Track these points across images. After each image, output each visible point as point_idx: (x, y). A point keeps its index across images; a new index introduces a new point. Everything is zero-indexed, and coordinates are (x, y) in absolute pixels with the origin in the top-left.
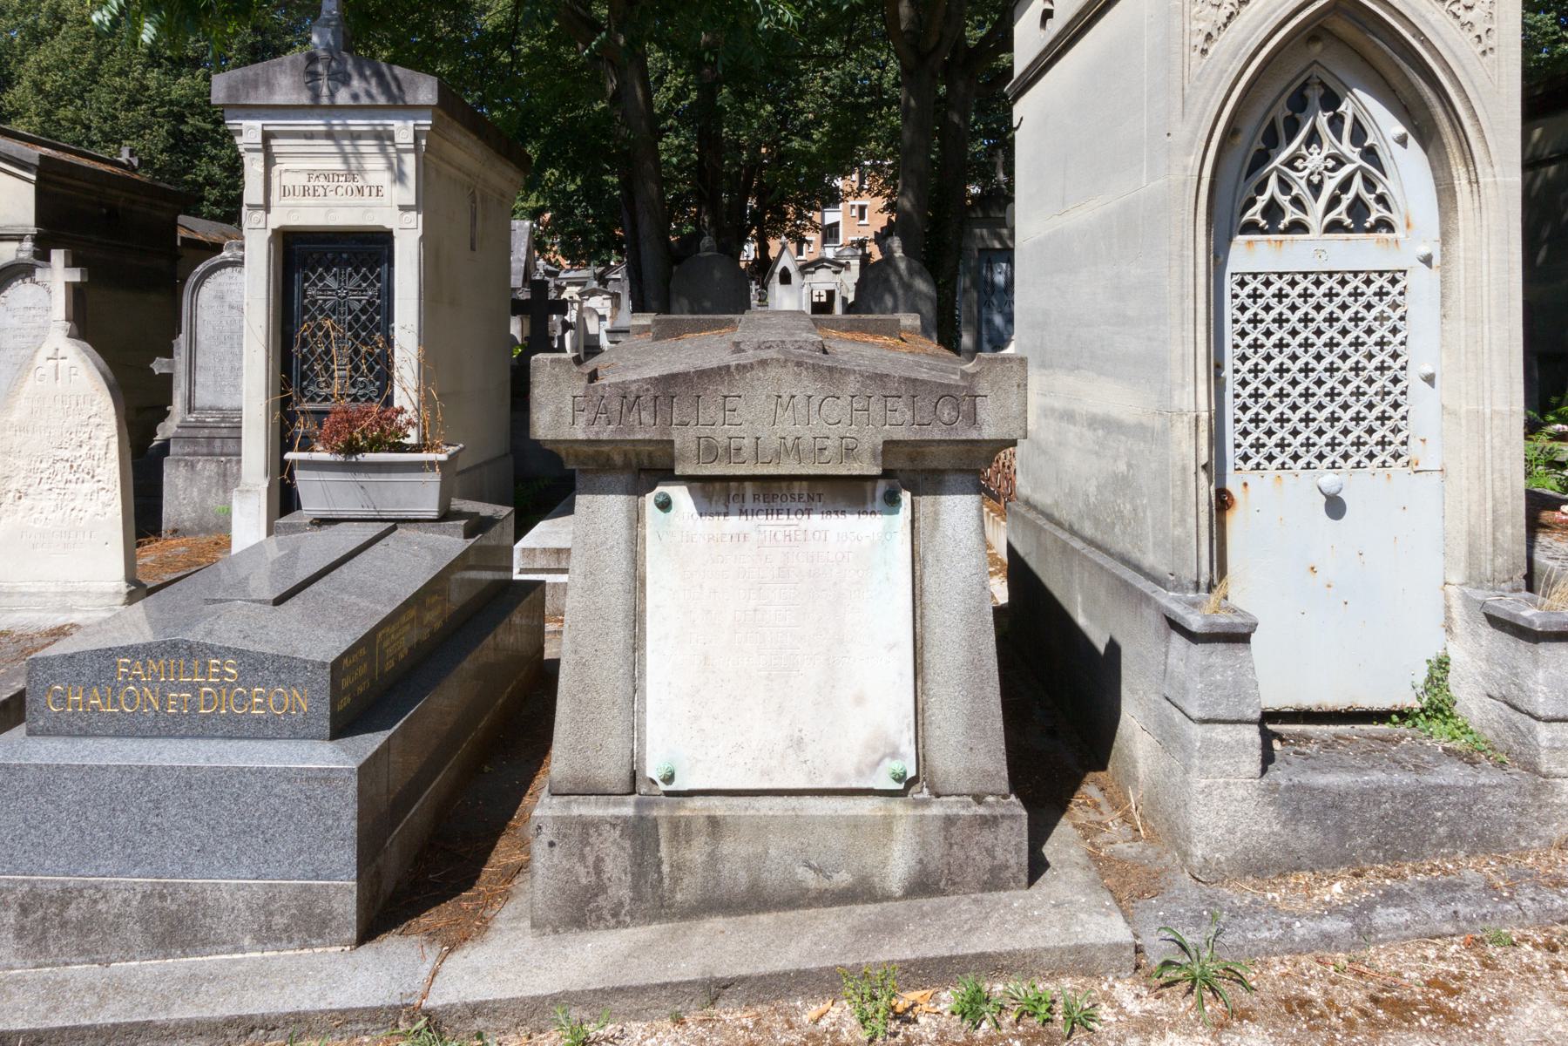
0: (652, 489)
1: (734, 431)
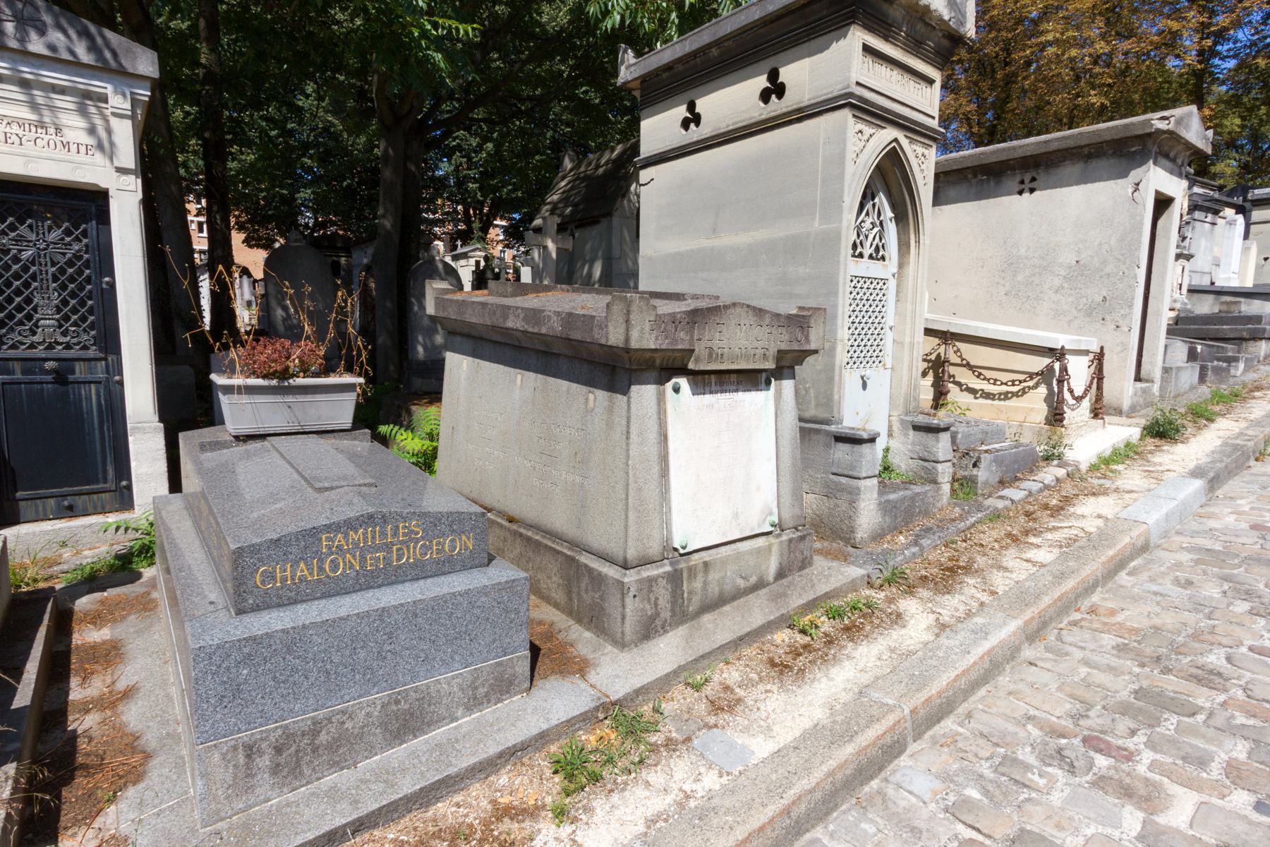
0: (668, 380)
1: (721, 344)
